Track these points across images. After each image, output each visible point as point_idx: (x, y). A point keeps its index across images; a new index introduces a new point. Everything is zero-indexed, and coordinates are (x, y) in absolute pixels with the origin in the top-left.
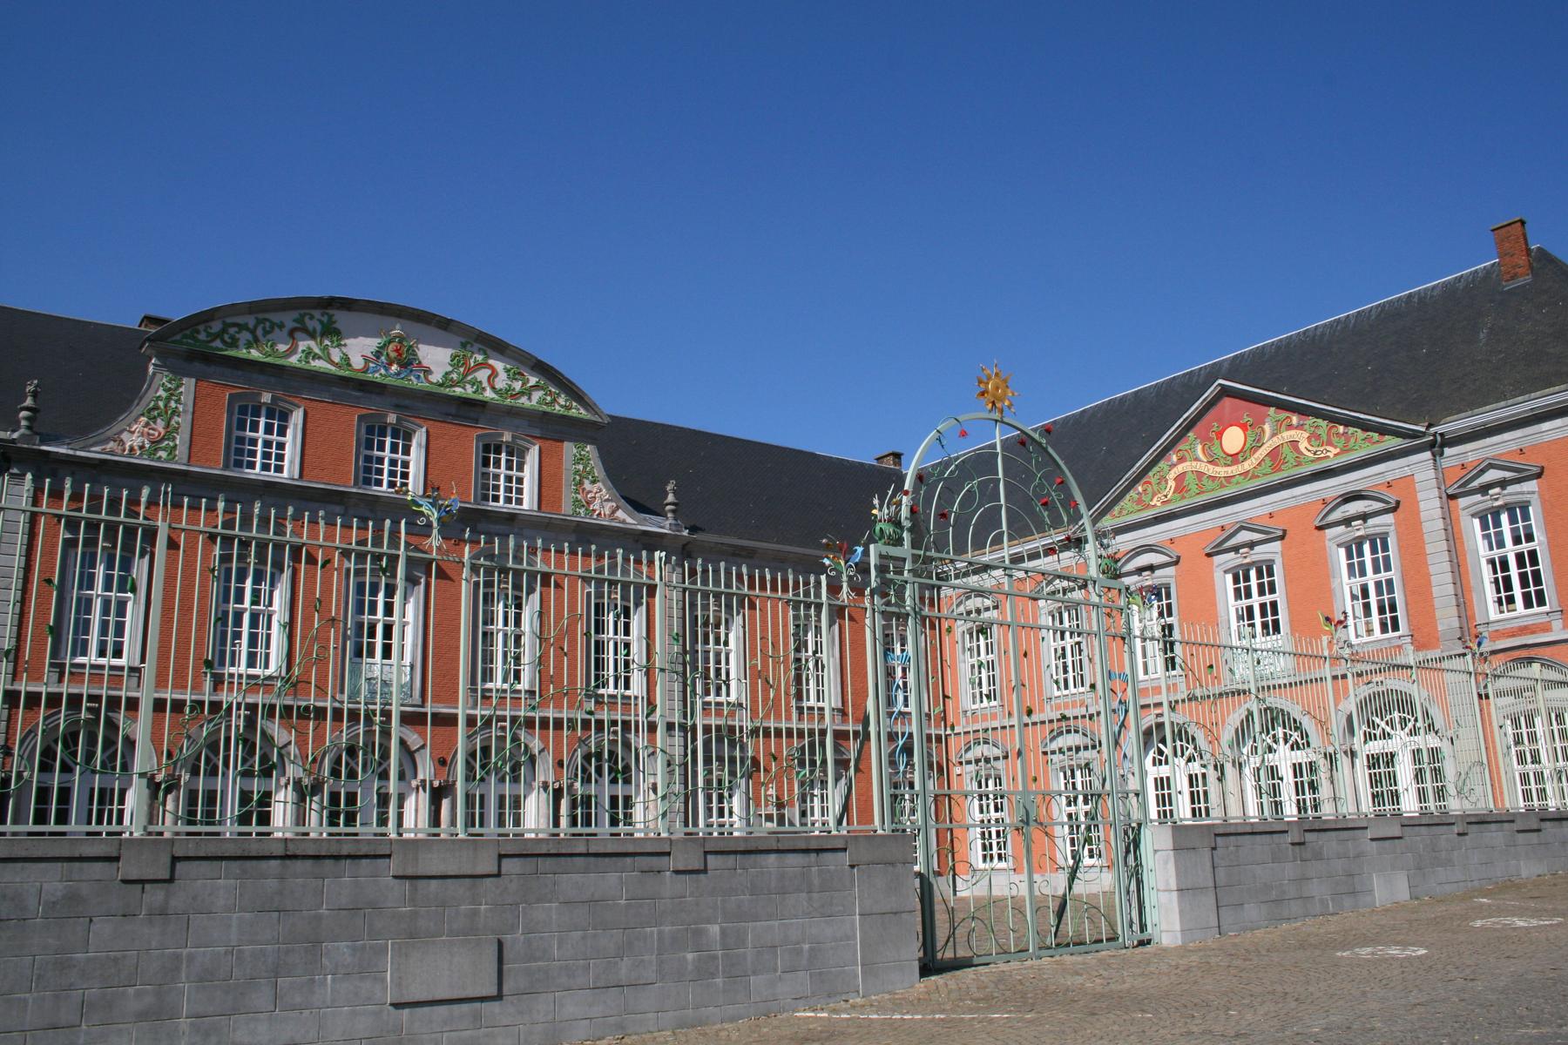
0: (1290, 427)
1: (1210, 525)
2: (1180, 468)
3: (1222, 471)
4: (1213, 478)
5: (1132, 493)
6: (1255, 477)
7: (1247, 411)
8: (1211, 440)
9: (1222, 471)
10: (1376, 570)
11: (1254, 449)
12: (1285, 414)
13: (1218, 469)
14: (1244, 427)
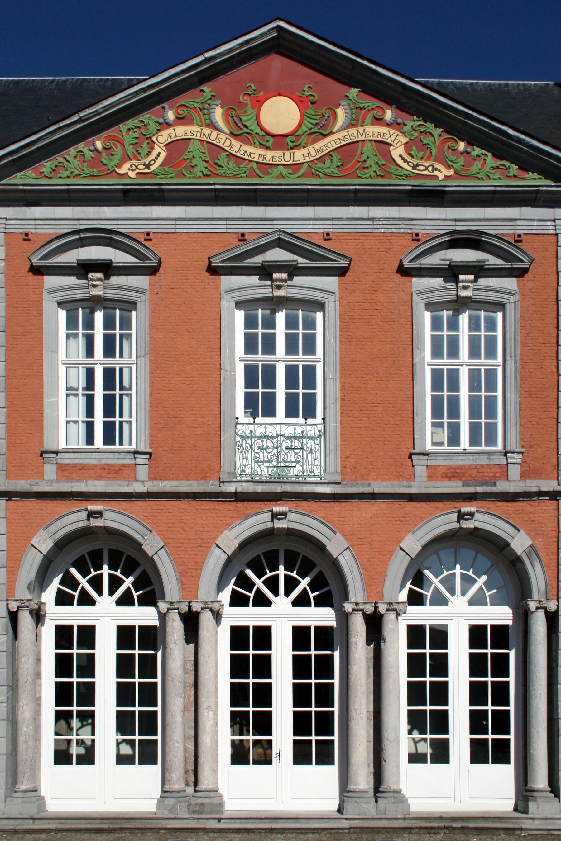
2: (180, 131)
3: (255, 153)
4: (238, 160)
9: (255, 153)
10: (474, 353)
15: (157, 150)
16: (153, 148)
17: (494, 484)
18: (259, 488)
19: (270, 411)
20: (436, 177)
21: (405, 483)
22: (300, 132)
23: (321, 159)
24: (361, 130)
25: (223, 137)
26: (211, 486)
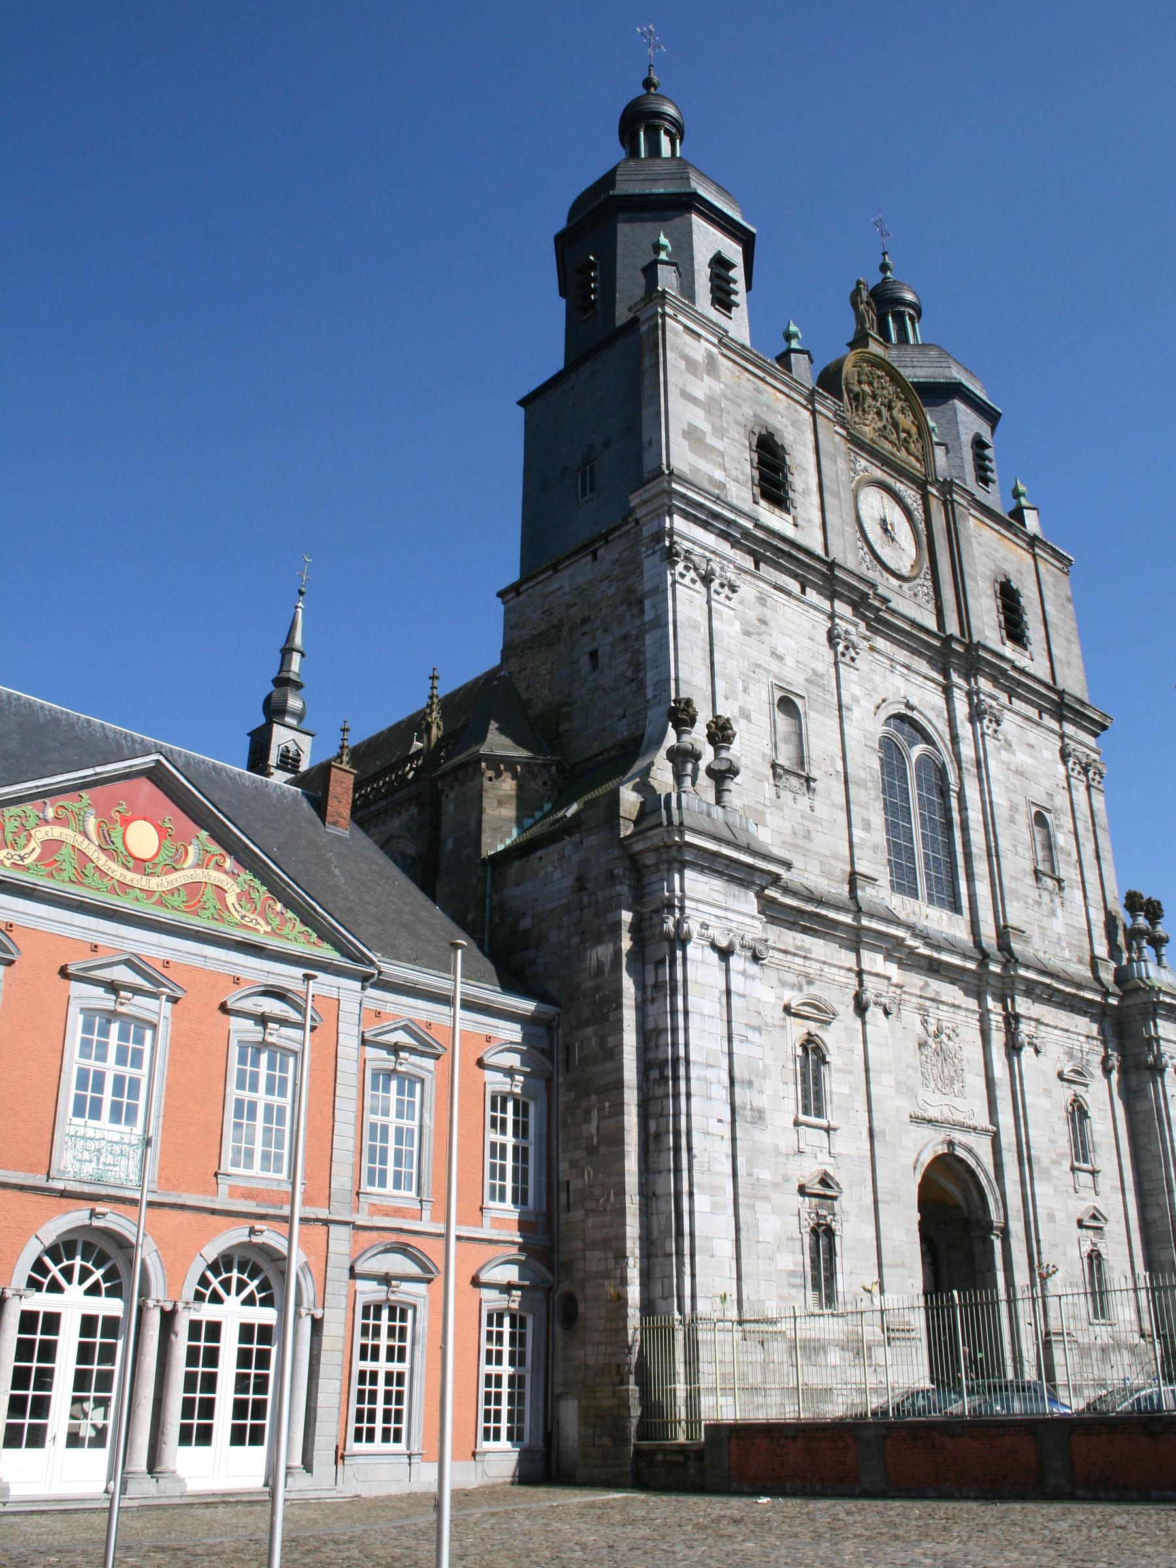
0: (219, 866)
1: (78, 934)
6: (161, 903)
7: (171, 814)
8: (114, 822)
9: (117, 871)
12: (215, 848)
13: (114, 866)
14: (162, 832)
15: (32, 844)
16: (29, 841)
17: (281, 1208)
18: (87, 1189)
19: (96, 1114)
20: (257, 930)
21: (209, 1198)
22: (156, 861)
23: (171, 892)
24: (205, 871)
25: (92, 846)
26: (39, 1180)
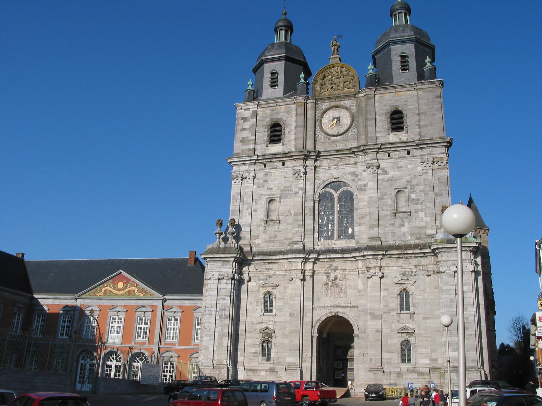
3: (116, 292)
5: (92, 291)
6: (123, 295)
9: (116, 292)
11: (124, 289)
